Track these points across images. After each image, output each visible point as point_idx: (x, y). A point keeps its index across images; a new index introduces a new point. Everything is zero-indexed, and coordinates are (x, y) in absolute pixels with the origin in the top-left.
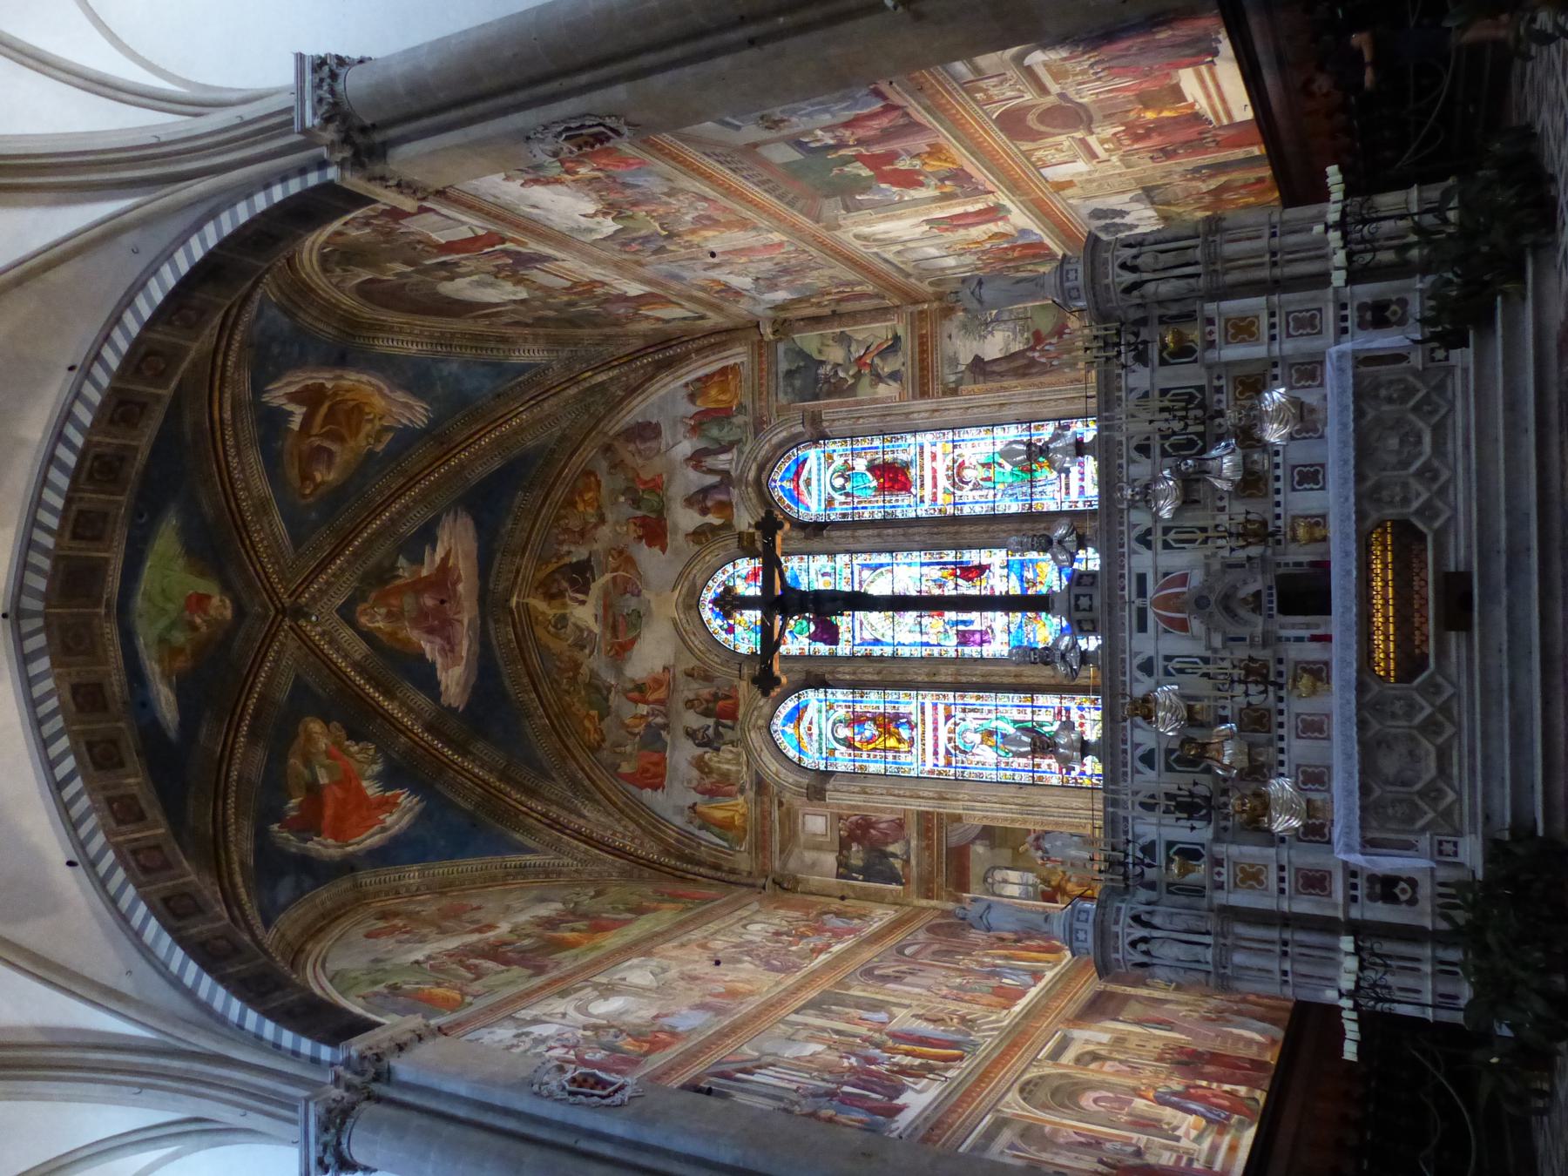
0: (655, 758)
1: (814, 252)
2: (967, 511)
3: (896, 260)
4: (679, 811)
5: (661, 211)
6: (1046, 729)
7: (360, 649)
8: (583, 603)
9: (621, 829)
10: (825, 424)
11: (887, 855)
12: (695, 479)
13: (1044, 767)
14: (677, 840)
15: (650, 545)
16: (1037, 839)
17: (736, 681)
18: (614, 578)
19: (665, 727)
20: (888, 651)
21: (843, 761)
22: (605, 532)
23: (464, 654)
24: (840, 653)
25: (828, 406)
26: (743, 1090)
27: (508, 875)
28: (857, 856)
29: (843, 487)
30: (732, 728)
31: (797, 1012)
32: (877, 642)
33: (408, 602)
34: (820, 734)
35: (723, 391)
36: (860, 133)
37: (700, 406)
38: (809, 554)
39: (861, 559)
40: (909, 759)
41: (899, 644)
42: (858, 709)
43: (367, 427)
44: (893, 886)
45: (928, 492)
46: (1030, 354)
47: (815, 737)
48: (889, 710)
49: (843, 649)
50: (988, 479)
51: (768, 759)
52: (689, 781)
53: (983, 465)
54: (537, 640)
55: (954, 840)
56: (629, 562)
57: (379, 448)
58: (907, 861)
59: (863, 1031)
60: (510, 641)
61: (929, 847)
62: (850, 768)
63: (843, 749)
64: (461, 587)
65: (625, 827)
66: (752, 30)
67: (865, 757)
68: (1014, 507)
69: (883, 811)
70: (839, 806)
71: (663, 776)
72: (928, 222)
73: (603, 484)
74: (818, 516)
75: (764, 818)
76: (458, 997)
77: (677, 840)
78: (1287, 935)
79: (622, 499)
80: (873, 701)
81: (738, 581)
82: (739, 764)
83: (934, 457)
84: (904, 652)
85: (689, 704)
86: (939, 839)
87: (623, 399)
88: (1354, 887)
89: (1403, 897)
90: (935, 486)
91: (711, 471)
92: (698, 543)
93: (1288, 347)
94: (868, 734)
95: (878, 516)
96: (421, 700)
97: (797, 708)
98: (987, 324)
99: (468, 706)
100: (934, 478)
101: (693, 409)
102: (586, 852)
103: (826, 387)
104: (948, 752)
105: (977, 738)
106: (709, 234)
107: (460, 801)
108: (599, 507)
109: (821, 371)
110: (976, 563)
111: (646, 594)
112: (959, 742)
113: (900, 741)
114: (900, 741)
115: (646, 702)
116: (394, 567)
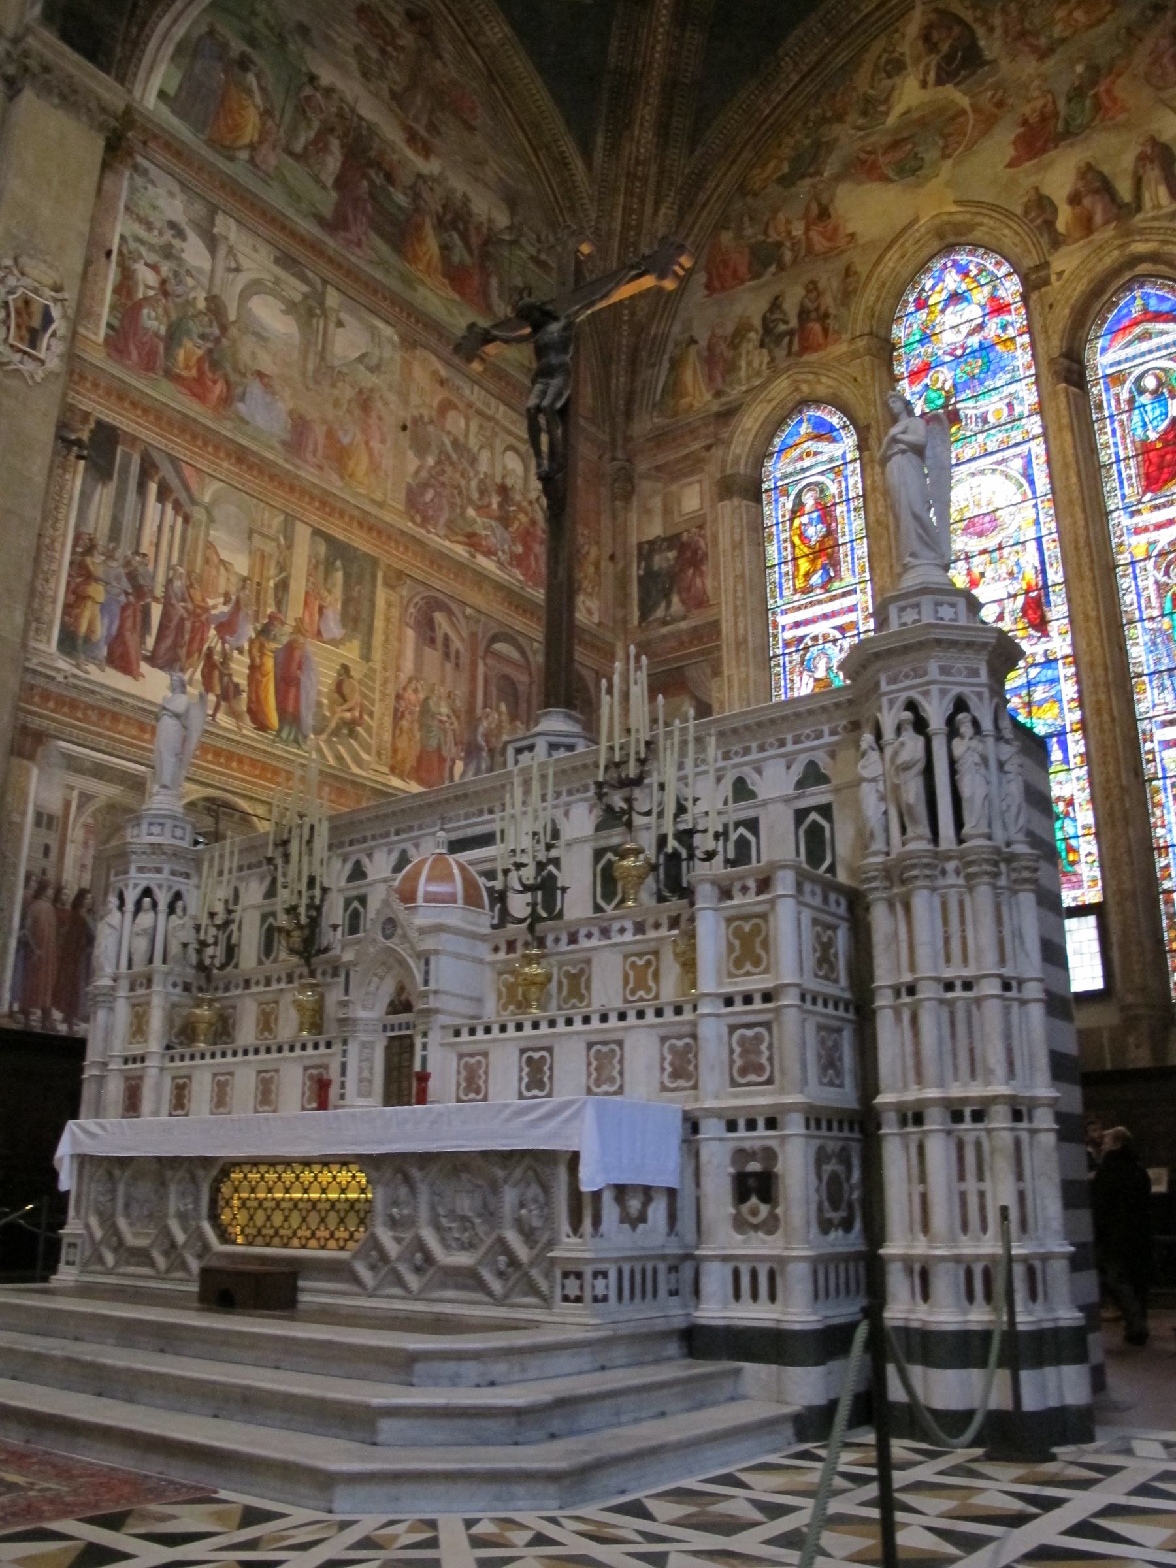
0: (743, 270)
2: (1125, 583)
8: (924, 84)
11: (667, 596)
17: (846, 336)
18: (963, 112)
21: (776, 511)
26: (120, 496)
27: (548, 148)
28: (664, 560)
29: (1142, 391)
30: (789, 354)
31: (317, 532)
34: (804, 470)
39: (1038, 449)
42: (839, 509)
44: (636, 613)
47: (799, 465)
48: (841, 549)
54: (865, 48)
55: (692, 673)
56: (989, 123)
58: (664, 622)
59: (295, 609)
62: (767, 522)
63: (789, 505)
67: (783, 536)
68: (1139, 653)
69: (716, 576)
70: (715, 521)
71: (723, 288)
76: (246, 140)
77: (655, 337)
81: (987, 289)
82: (749, 379)
85: (812, 287)
86: (693, 655)
90: (1158, 527)
92: (1026, 213)
93: (712, 1033)
94: (811, 531)
95: (1104, 457)
97: (832, 429)
104: (801, 639)
107: (614, 44)
111: (949, 163)
113: (808, 575)
114: (808, 575)
115: (807, 229)
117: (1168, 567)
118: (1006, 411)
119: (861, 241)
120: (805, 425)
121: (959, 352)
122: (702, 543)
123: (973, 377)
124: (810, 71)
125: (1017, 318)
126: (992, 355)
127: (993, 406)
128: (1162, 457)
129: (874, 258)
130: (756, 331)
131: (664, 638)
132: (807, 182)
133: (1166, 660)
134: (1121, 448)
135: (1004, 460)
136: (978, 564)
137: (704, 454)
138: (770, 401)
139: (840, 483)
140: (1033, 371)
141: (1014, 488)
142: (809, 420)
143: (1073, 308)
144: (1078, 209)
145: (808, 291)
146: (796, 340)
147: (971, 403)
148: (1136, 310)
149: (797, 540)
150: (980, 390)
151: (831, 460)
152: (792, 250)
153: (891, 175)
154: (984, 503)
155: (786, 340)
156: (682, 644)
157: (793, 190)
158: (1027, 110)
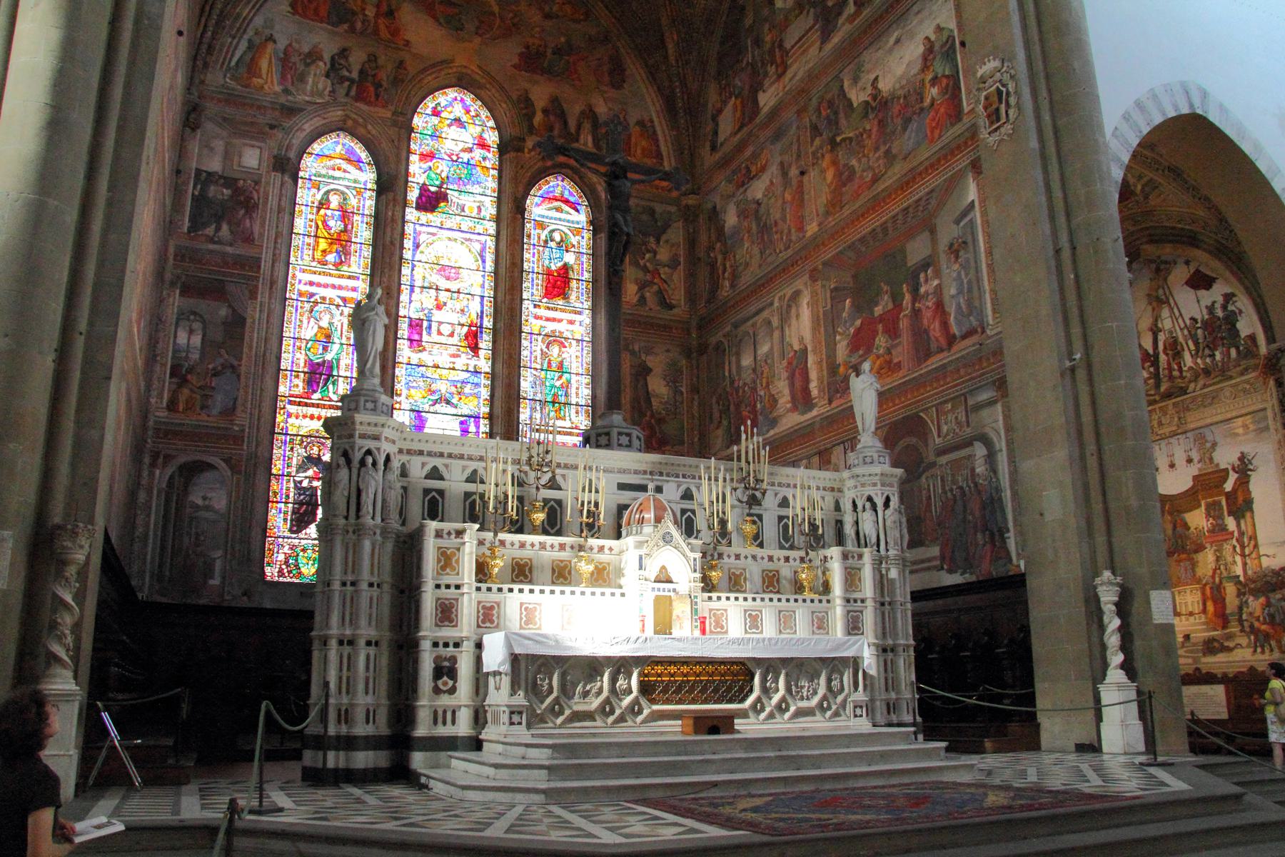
0: (323, 12)
1: (784, 255)
2: (525, 343)
3: (759, 319)
4: (269, 23)
5: (868, 143)
6: (331, 387)
12: (574, 110)
13: (296, 381)
14: (239, 15)
15: (521, 55)
16: (232, 367)
18: (493, 14)
19: (352, 29)
20: (407, 254)
21: (306, 195)
22: (535, 17)
24: (408, 210)
28: (220, 193)
29: (552, 240)
30: (347, 95)
32: (417, 246)
34: (334, 178)
35: (643, 150)
36: (927, 315)
37: (635, 130)
38: (499, 198)
39: (491, 244)
40: (307, 259)
41: (414, 266)
45: (542, 312)
46: (648, 414)
47: (331, 173)
48: (353, 247)
49: (411, 214)
50: (549, 363)
51: (317, 122)
52: (298, 42)
53: (561, 363)
55: (231, 288)
58: (211, 240)
61: (226, 264)
63: (319, 197)
66: (1066, 254)
67: (310, 217)
68: (526, 385)
69: (263, 225)
70: (268, 183)
71: (305, 16)
72: (804, 351)
74: (531, 213)
75: (259, 108)
78: (386, 587)
79: (563, 39)
80: (363, 233)
81: (479, 129)
82: (312, 94)
83: (571, 322)
84: (406, 270)
86: (232, 275)
88: (446, 645)
89: (440, 683)
90: (548, 319)
91: (579, 127)
94: (331, 223)
97: (360, 161)
98: (675, 382)
100: (554, 320)
101: (632, 121)
104: (312, 295)
105: (324, 324)
106: (830, 175)
108: (557, 16)
109: (652, 240)
110: (481, 345)
111: (479, 39)
112: (320, 307)
115: (377, 16)
117: (549, 344)
118: (476, 210)
120: (340, 147)
121: (455, 158)
122: (256, 198)
123: (460, 179)
125: (492, 158)
126: (474, 171)
127: (469, 202)
129: (422, 67)
130: (325, 64)
131: (211, 251)
133: (539, 395)
134: (536, 266)
135: (469, 240)
136: (444, 296)
139: (359, 199)
140: (496, 195)
141: (473, 260)
142: (344, 145)
146: (354, 88)
147: (456, 194)
148: (558, 192)
149: (321, 226)
150: (463, 189)
151: (355, 181)
152: (363, 23)
153: (442, 20)
154: (453, 260)
155: (347, 83)
156: (226, 264)
158: (531, 41)
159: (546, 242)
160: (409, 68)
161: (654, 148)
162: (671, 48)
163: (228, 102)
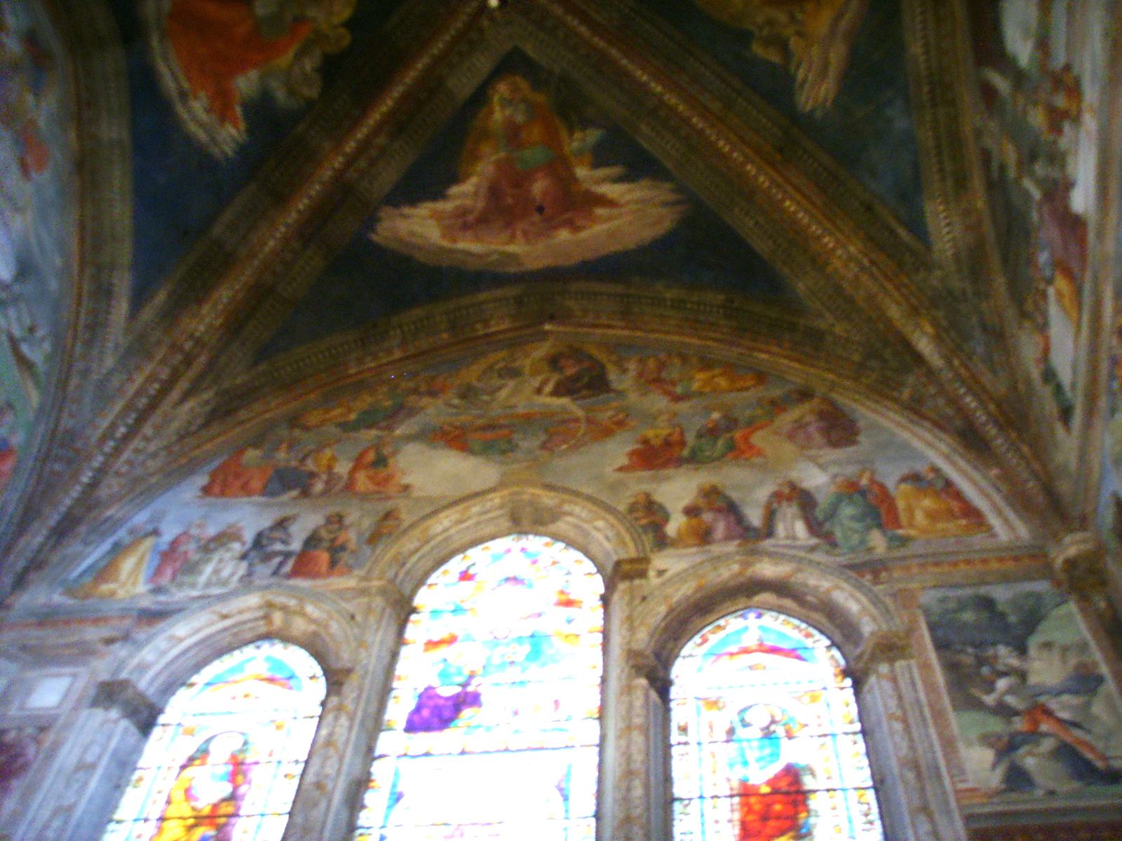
0: (256, 484)
7: (462, 85)
9: (152, 448)
10: (884, 668)
15: (633, 453)
18: (577, 420)
23: (461, 245)
25: (925, 666)
29: (745, 724)
30: (275, 573)
33: (534, 154)
35: (932, 516)
43: (781, 16)
57: (757, 49)
60: (486, 323)
64: (564, 235)
65: (154, 455)
71: (223, 493)
73: (745, 394)
82: (208, 585)
85: (337, 521)
87: (895, 400)
91: (770, 516)
96: (388, 176)
99: (380, 251)
101: (891, 484)
102: (120, 390)
103: (967, 659)
107: (228, 216)
109: (1002, 650)
116: (585, 124)
119: (416, 494)
124: (414, 356)
128: (769, 806)
129: (428, 510)
130: (244, 544)
132: (374, 432)
137: (101, 647)
138: (225, 617)
143: (671, 610)
144: (694, 521)
145: (329, 520)
148: (750, 640)
152: (327, 482)
155: (277, 560)
157: (353, 435)
158: (650, 433)
159: (731, 732)
160: (403, 516)
161: (955, 505)
162: (924, 345)
163: (41, 624)
